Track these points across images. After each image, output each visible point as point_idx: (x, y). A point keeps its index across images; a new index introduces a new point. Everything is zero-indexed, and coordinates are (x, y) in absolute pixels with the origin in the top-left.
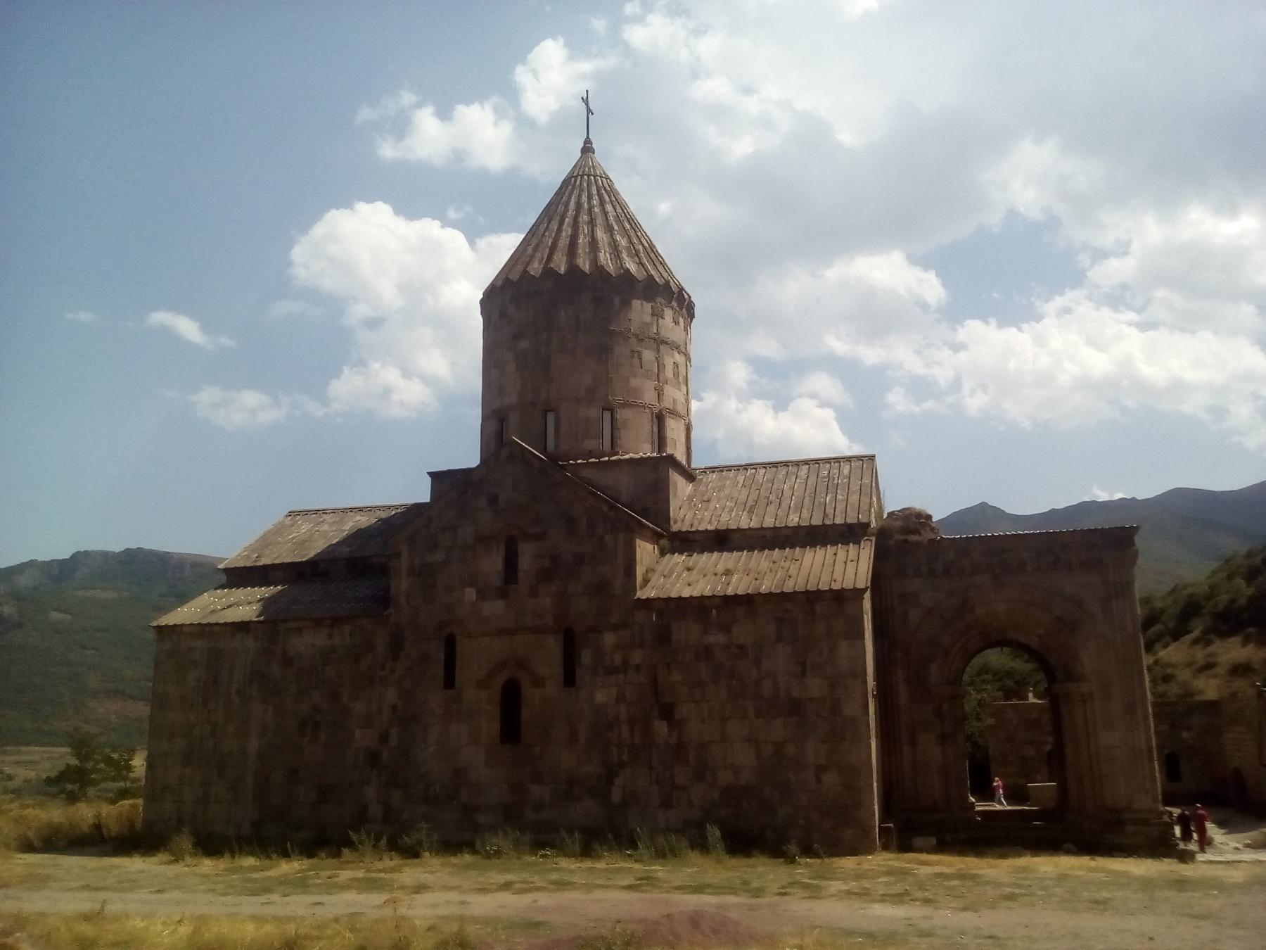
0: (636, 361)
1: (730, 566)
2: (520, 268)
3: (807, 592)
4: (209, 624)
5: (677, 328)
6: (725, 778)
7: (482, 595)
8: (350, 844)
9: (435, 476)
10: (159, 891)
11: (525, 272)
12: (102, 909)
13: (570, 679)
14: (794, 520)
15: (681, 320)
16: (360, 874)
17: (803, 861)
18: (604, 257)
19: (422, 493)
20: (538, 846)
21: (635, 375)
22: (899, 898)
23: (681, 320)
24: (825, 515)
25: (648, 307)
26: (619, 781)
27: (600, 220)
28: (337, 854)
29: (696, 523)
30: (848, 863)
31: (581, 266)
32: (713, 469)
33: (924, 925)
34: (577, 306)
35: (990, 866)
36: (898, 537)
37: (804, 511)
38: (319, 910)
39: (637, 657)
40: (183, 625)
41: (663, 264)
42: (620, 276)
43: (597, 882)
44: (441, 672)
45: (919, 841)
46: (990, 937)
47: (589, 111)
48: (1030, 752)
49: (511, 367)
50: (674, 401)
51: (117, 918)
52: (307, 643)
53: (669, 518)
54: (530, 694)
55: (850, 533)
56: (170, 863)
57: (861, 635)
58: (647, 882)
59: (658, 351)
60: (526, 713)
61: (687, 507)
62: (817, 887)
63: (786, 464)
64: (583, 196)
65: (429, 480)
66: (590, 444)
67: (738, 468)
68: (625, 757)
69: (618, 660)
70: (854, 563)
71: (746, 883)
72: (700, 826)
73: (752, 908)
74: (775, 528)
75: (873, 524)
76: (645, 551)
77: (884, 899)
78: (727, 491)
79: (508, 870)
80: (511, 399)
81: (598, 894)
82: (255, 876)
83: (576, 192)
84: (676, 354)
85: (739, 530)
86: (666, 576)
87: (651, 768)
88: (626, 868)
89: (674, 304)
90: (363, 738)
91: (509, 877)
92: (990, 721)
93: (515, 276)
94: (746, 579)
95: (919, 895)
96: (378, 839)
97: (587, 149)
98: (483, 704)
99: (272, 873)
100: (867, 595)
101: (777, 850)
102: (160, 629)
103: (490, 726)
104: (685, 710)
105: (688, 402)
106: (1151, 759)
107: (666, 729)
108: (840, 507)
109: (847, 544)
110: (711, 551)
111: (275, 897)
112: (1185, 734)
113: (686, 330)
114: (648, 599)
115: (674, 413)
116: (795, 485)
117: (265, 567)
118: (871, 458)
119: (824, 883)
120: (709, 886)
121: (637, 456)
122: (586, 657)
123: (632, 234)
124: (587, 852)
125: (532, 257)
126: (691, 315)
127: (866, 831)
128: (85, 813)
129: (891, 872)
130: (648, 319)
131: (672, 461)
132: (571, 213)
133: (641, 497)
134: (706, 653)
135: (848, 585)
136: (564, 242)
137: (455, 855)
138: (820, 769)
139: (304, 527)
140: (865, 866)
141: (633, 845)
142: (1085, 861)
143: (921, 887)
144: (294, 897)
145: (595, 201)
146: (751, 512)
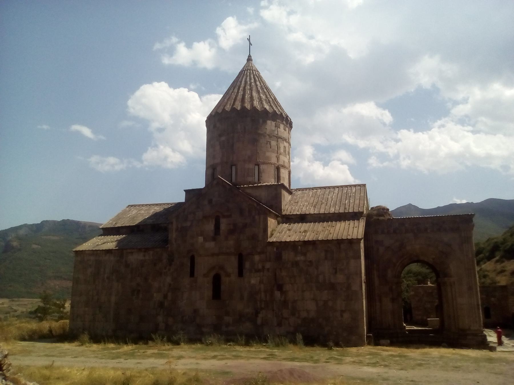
0: (268, 145)
1: (306, 229)
2: (222, 107)
3: (338, 240)
4: (96, 250)
5: (285, 132)
6: (304, 314)
7: (205, 240)
8: (152, 339)
9: (187, 192)
10: (75, 357)
11: (224, 110)
12: (53, 364)
13: (241, 274)
14: (332, 210)
15: (287, 129)
16: (156, 351)
17: (335, 349)
18: (256, 103)
19: (181, 198)
20: (227, 341)
22: (374, 365)
23: (287, 129)
24: (345, 208)
25: (273, 123)
26: (260, 315)
27: (254, 88)
28: (146, 343)
29: (292, 211)
30: (354, 350)
31: (247, 107)
32: (299, 190)
33: (385, 376)
34: (245, 123)
35: (412, 352)
36: (375, 217)
37: (337, 207)
38: (139, 365)
39: (268, 265)
40: (85, 251)
41: (280, 106)
42: (262, 111)
43: (251, 356)
44: (189, 270)
45: (382, 341)
46: (412, 381)
47: (250, 44)
49: (218, 148)
50: (284, 162)
51: (58, 368)
52: (135, 258)
53: (281, 210)
54: (225, 280)
55: (355, 216)
56: (79, 346)
57: (359, 257)
58: (272, 356)
59: (278, 141)
60: (223, 287)
61: (288, 205)
62: (341, 359)
63: (329, 187)
64: (247, 79)
65: (185, 193)
66: (250, 179)
67: (310, 189)
68: (263, 306)
69: (260, 267)
70: (357, 228)
71: (312, 357)
72: (294, 334)
73: (314, 368)
74: (325, 214)
75: (365, 212)
76: (272, 222)
77: (368, 365)
78: (305, 198)
79: (215, 351)
80: (218, 160)
81: (252, 361)
82: (114, 351)
83: (245, 77)
84: (285, 143)
85: (310, 214)
86: (280, 233)
87: (273, 310)
88: (264, 350)
89: (284, 122)
90: (157, 297)
91: (216, 353)
92: (412, 293)
93: (220, 111)
94: (313, 234)
95: (383, 363)
96: (163, 338)
97: (249, 59)
98: (206, 284)
99: (121, 350)
100: (362, 241)
101: (324, 344)
102: (76, 252)
103: (208, 293)
104: (287, 287)
105: (289, 162)
106: (479, 309)
108: (351, 205)
109: (354, 220)
110: (298, 223)
111: (122, 360)
112: (493, 299)
113: (289, 133)
114: (273, 242)
115: (284, 167)
116: (334, 195)
117: (119, 227)
118: (364, 185)
119: (344, 358)
120: (297, 358)
121: (269, 184)
122: (247, 265)
123: (267, 94)
124: (247, 344)
125: (227, 103)
126: (291, 127)
127: (361, 337)
128: (46, 325)
129: (371, 354)
130: (274, 128)
131: (283, 186)
132: (243, 85)
133: (270, 201)
134: (296, 264)
135: (355, 237)
136: (240, 97)
137: (194, 344)
138: (342, 312)
139: (134, 212)
140: (361, 351)
141: (266, 342)
142: (451, 350)
143: (384, 360)
144: (129, 360)
145: (253, 81)
146: (315, 207)
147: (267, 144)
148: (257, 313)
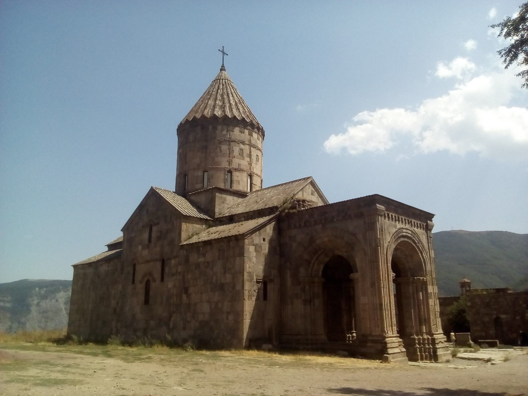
0: (218, 150)
5: (243, 135)
6: (201, 317)
13: (162, 279)
15: (246, 132)
21: (217, 156)
26: (172, 319)
36: (287, 211)
42: (211, 118)
45: (265, 346)
48: (487, 319)
53: (214, 213)
54: (153, 285)
59: (230, 145)
60: (151, 293)
66: (199, 186)
69: (175, 271)
84: (242, 146)
97: (223, 69)
103: (142, 298)
104: (191, 290)
105: (250, 164)
107: (185, 298)
110: (229, 224)
122: (167, 270)
127: (241, 340)
134: (198, 265)
138: (228, 313)
147: (216, 149)
148: (170, 317)
